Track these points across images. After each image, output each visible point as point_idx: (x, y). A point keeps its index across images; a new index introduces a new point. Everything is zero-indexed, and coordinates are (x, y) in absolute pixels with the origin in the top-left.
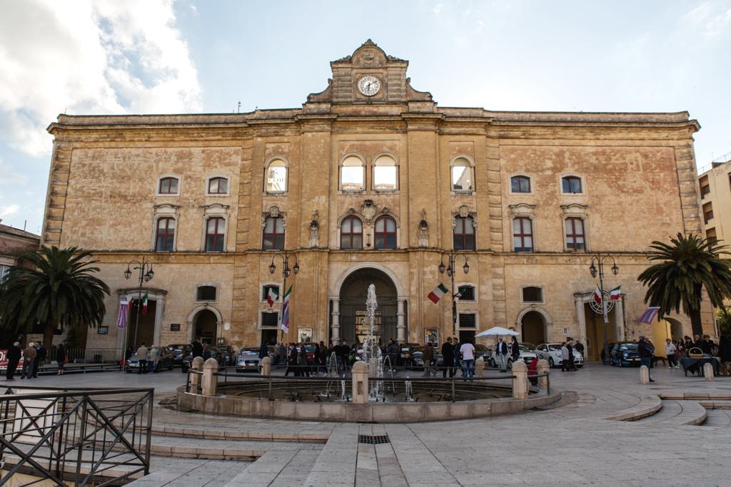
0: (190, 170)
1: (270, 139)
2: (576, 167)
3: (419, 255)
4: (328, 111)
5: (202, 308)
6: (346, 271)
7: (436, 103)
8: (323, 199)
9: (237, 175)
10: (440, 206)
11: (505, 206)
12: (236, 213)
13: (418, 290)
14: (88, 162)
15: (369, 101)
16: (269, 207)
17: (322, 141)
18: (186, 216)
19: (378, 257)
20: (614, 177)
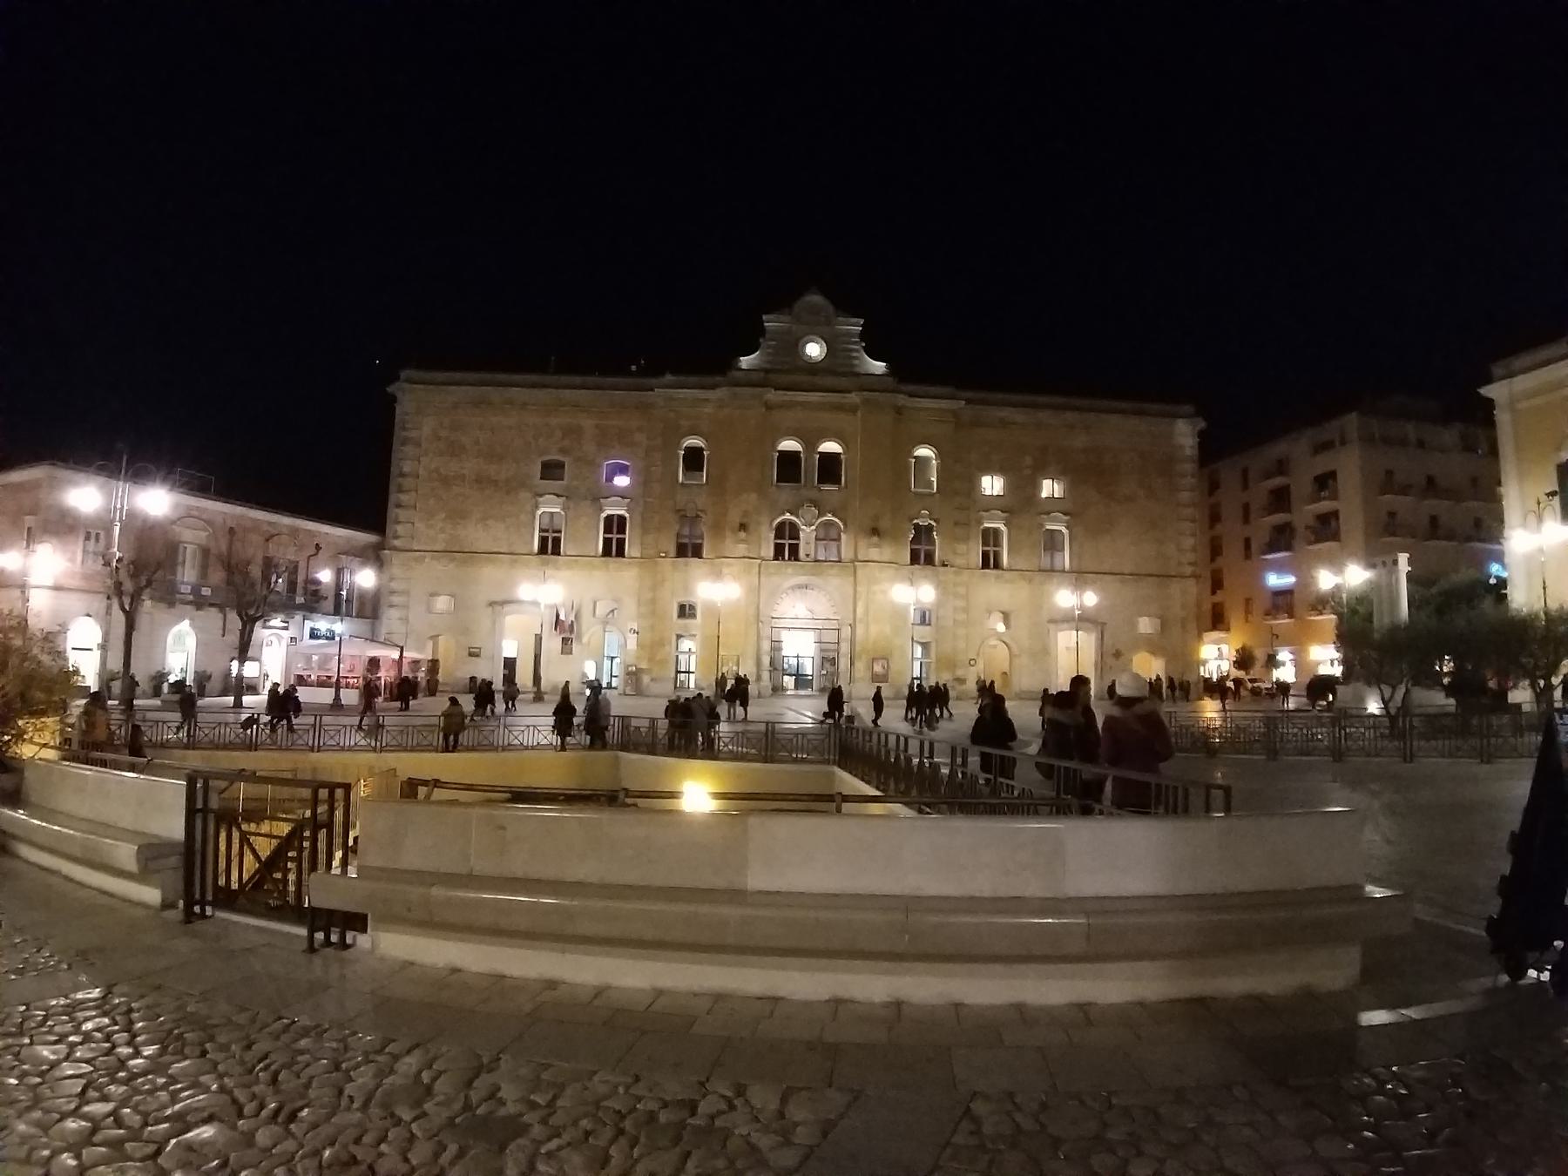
14: (443, 433)
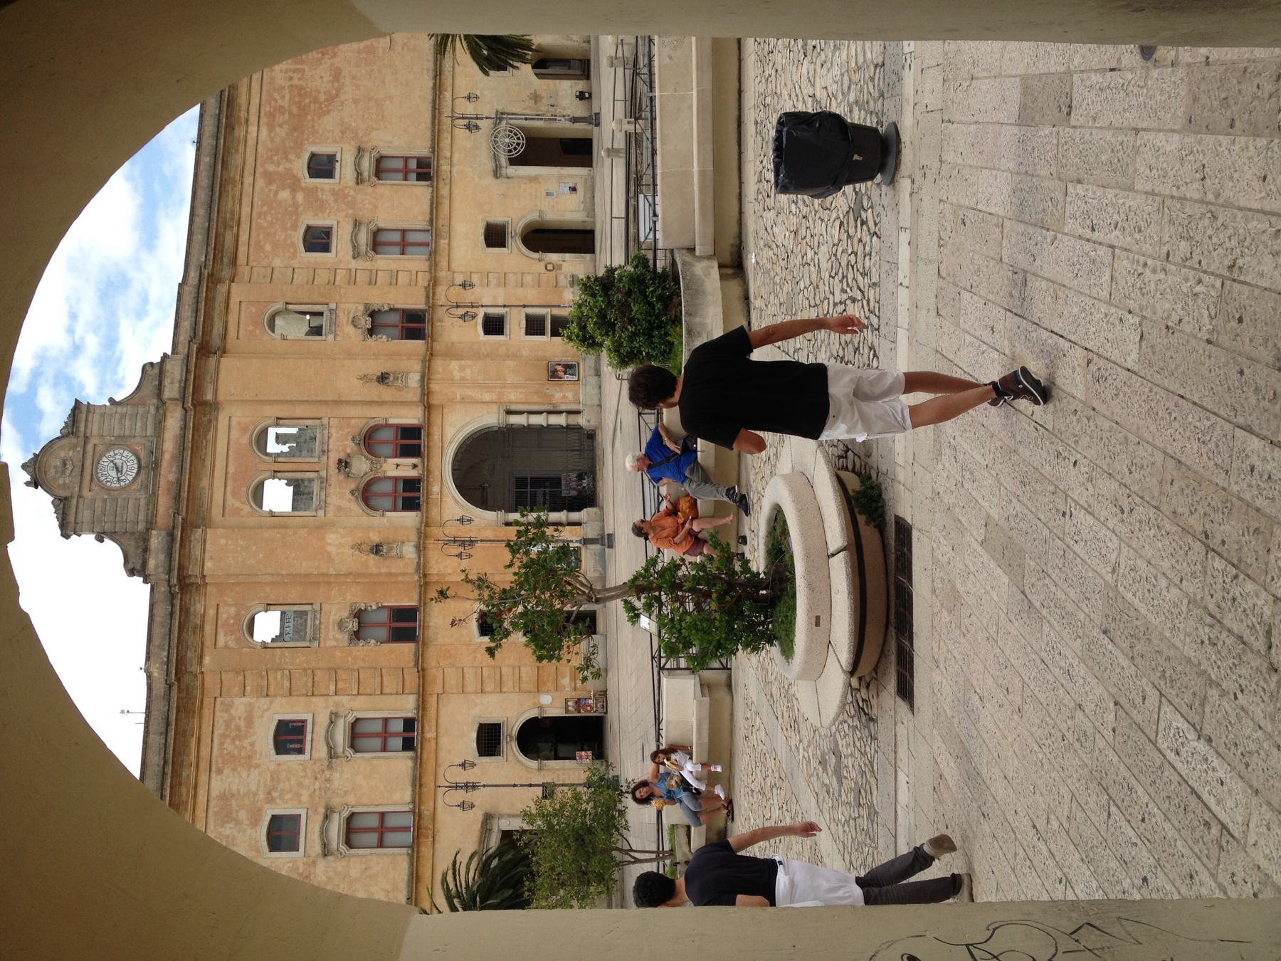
0: (256, 794)
1: (208, 641)
2: (292, 156)
3: (435, 387)
4: (164, 533)
5: (514, 746)
6: (457, 502)
7: (165, 356)
8: (331, 537)
9: (271, 703)
10: (350, 355)
11: (354, 264)
12: (345, 700)
13: (489, 389)
15: (149, 466)
16: (339, 636)
17: (223, 541)
18: (346, 793)
19: (436, 452)
20: (312, 105)
